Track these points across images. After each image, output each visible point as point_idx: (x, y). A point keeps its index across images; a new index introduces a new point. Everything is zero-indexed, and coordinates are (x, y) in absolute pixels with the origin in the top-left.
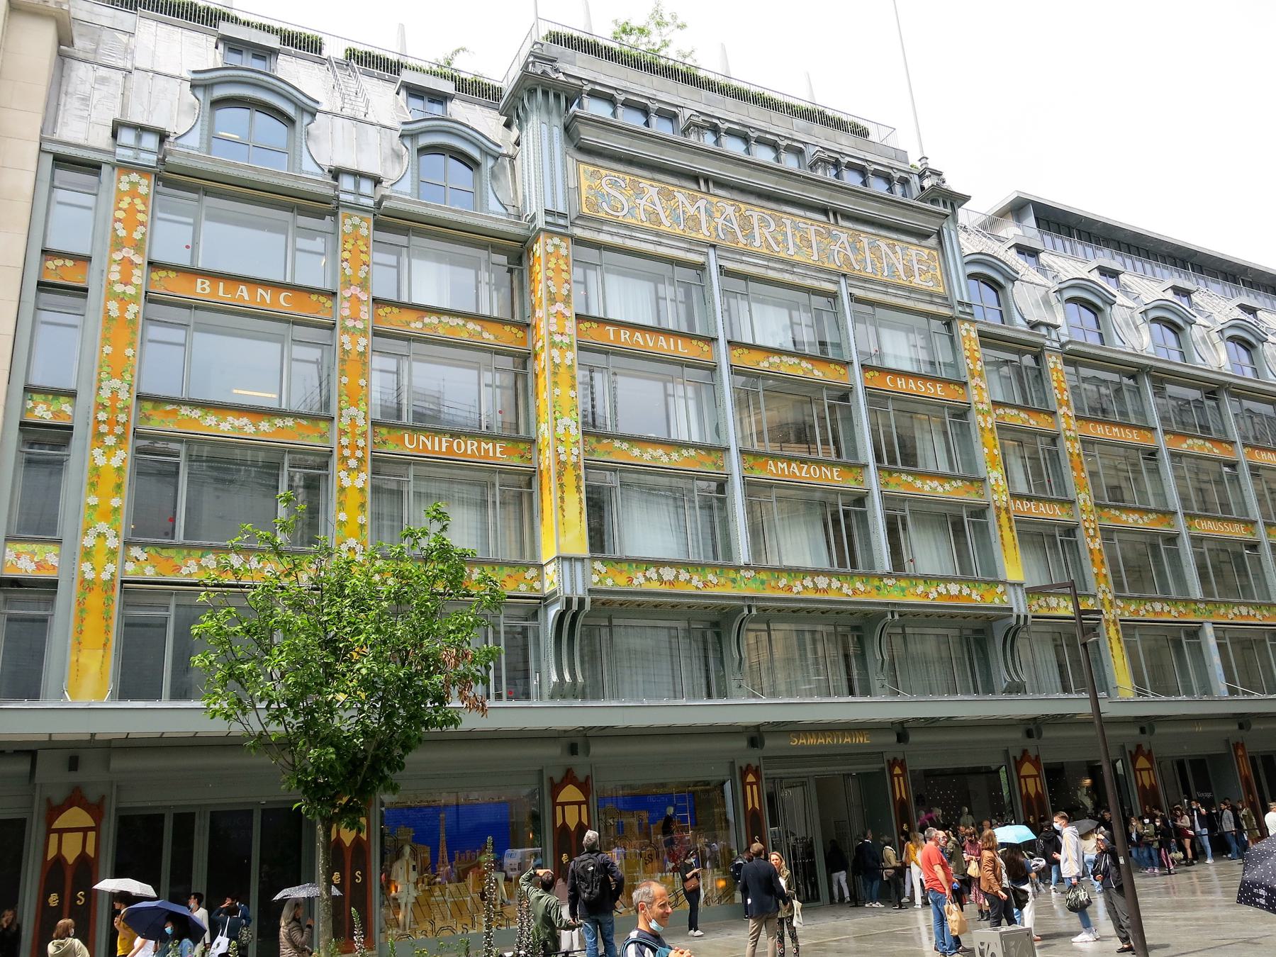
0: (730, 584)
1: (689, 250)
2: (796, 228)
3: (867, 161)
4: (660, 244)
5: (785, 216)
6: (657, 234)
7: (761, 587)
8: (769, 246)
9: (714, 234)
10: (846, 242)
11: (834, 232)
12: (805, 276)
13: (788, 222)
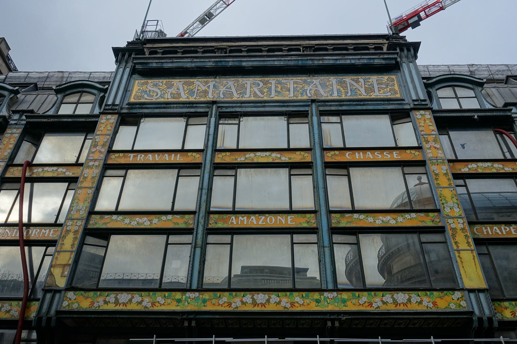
0: (175, 303)
7: (202, 304)
8: (255, 94)
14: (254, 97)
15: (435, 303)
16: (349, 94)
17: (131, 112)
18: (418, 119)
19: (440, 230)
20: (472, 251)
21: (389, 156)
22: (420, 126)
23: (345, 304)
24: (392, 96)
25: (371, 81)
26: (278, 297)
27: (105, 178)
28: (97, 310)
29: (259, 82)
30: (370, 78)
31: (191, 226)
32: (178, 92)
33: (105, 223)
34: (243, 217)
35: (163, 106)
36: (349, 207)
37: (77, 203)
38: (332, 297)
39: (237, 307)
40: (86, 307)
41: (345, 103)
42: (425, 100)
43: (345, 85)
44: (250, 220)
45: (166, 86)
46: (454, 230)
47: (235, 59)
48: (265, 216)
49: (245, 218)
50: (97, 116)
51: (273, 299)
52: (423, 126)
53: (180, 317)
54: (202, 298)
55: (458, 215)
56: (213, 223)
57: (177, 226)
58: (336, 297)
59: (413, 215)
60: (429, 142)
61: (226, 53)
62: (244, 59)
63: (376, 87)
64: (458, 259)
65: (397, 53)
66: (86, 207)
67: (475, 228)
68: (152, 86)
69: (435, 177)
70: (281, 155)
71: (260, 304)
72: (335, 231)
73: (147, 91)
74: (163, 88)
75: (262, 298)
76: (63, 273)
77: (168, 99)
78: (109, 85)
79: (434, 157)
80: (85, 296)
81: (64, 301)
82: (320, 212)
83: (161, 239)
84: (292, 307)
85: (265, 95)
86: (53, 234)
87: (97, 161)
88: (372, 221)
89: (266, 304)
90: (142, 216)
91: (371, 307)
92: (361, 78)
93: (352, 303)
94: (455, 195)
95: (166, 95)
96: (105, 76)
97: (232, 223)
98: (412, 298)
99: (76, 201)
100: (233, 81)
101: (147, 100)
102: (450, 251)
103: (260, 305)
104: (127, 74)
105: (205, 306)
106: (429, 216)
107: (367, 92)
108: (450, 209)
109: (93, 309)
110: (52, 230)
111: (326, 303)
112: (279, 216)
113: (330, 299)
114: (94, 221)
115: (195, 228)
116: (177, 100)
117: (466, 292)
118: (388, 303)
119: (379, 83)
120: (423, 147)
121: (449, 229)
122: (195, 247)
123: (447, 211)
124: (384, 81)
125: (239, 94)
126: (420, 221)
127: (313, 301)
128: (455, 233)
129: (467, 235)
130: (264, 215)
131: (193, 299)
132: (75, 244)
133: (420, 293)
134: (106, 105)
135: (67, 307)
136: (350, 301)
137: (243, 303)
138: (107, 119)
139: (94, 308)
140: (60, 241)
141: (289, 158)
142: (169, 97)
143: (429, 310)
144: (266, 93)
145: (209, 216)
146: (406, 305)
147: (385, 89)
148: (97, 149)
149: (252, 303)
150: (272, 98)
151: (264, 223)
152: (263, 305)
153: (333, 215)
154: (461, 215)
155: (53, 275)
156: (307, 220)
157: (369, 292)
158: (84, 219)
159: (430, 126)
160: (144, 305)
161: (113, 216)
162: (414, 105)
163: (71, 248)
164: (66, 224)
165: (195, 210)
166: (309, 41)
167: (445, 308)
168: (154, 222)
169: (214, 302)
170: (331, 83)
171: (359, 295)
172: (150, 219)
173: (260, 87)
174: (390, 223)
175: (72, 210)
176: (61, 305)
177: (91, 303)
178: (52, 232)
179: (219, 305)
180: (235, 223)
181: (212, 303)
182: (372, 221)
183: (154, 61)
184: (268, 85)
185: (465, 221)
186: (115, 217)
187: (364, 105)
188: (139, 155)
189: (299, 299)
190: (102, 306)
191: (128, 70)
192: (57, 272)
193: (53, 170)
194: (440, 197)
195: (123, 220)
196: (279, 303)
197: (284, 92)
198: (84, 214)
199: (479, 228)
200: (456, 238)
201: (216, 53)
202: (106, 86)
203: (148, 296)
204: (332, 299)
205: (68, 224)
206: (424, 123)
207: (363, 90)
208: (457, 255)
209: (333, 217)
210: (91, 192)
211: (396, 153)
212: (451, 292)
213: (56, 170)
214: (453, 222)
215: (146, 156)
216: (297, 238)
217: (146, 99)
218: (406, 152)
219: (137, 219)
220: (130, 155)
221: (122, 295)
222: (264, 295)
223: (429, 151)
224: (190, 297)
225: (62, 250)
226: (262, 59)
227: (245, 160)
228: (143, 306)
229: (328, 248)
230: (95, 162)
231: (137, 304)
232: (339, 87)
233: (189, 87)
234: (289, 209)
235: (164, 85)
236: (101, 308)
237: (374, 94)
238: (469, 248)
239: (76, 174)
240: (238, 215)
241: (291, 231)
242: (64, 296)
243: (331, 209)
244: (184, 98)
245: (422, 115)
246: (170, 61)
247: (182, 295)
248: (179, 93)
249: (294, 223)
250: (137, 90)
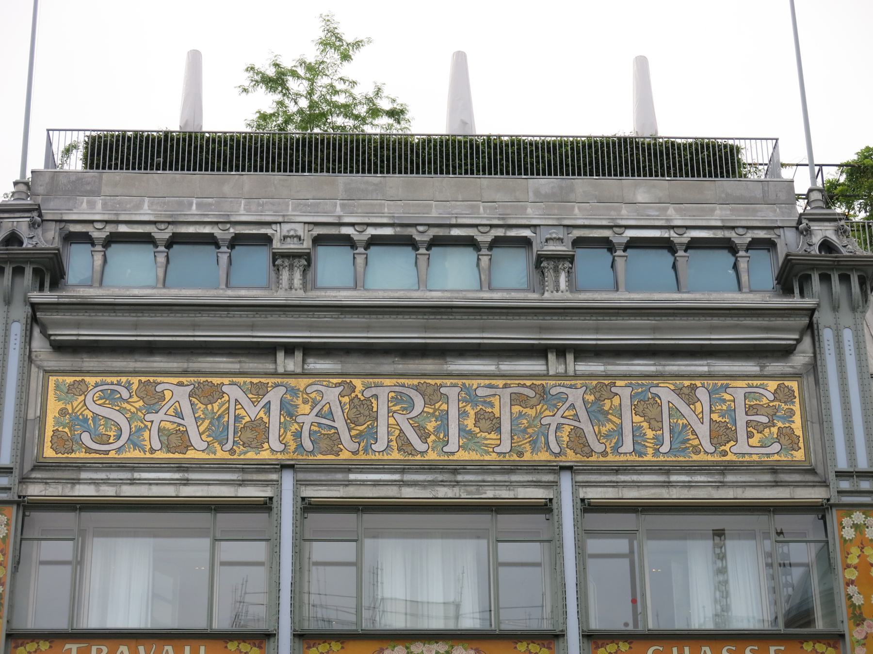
1: (242, 483)
2: (470, 397)
3: (673, 227)
4: (186, 482)
5: (448, 382)
6: (180, 467)
8: (405, 444)
9: (293, 446)
10: (579, 404)
11: (553, 391)
12: (480, 484)
13: (453, 393)
14: (399, 450)
16: (665, 448)
18: (845, 540)
22: (848, 566)
24: (783, 459)
25: (727, 397)
29: (413, 393)
30: (727, 386)
32: (179, 425)
45: (141, 403)
52: (855, 568)
63: (742, 419)
68: (101, 398)
73: (86, 420)
74: (133, 410)
77: (152, 451)
85: (430, 444)
92: (703, 386)
95: (146, 434)
101: (93, 455)
104: (17, 347)
116: (181, 456)
119: (752, 406)
124: (765, 401)
125: (356, 436)
142: (157, 445)
144: (433, 437)
147: (767, 430)
150: (451, 458)
170: (616, 401)
173: (414, 414)
184: (437, 405)
197: (484, 434)
206: (859, 556)
207: (703, 431)
217: (89, 450)
218: (802, 647)
220: (68, 646)
232: (637, 419)
233: (209, 407)
235: (135, 398)
245: (856, 526)
248: (182, 429)
250: (57, 415)
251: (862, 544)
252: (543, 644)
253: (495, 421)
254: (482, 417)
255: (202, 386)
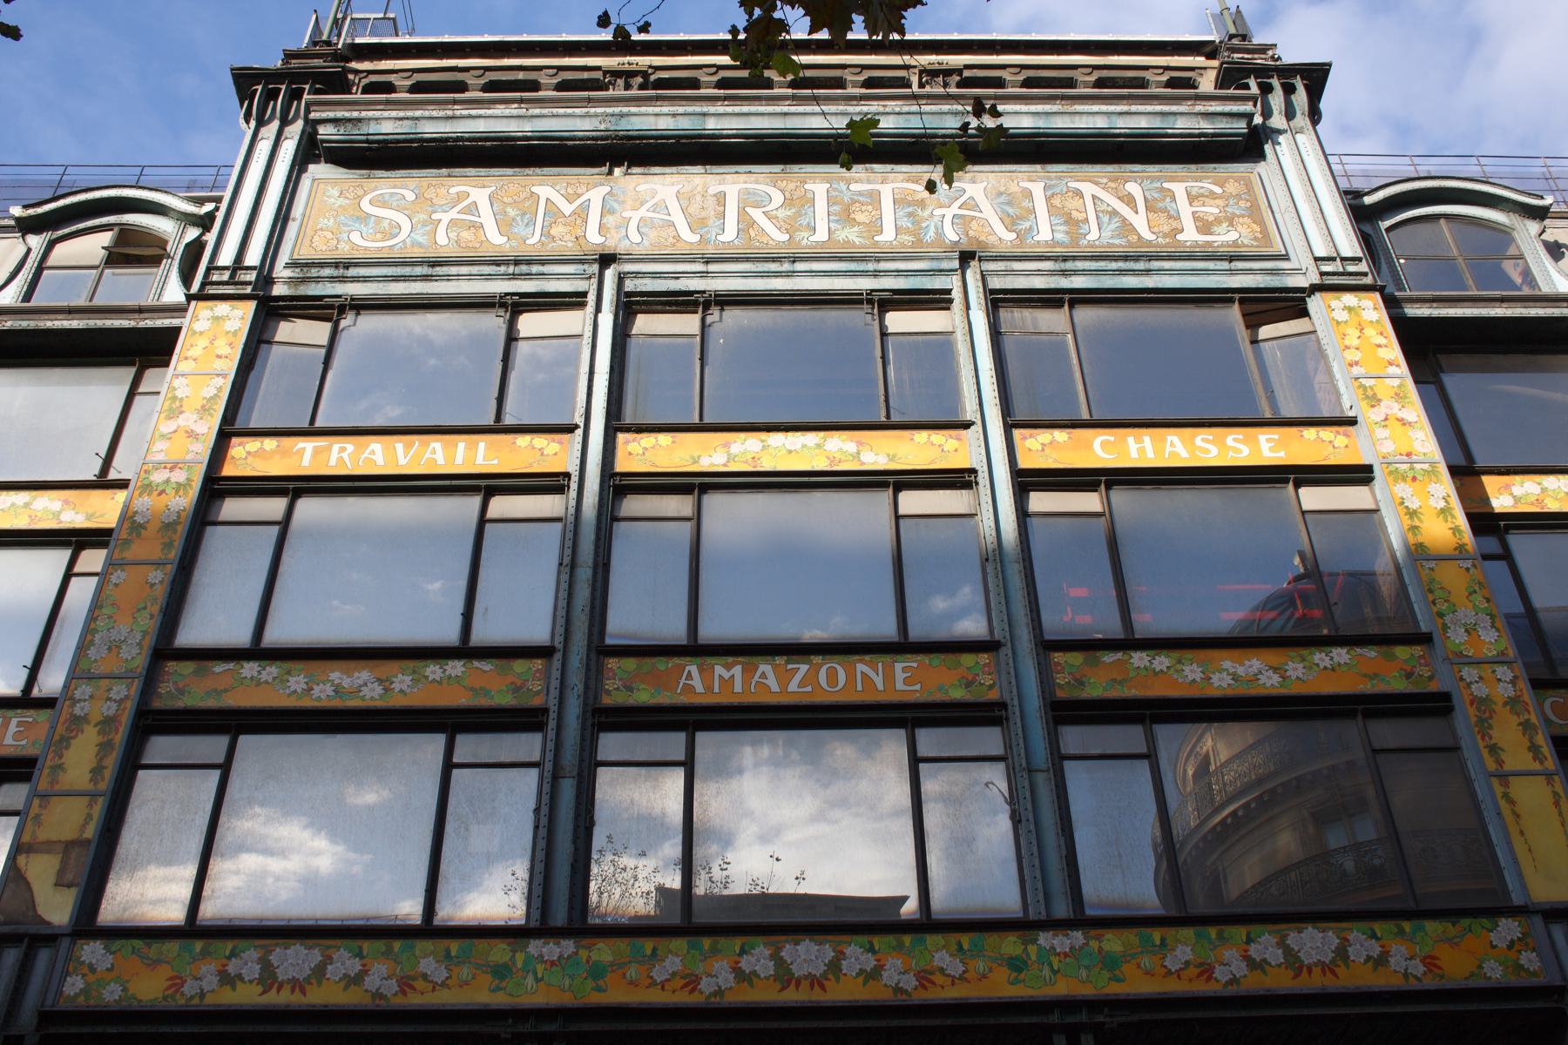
0: (486, 979)
7: (590, 984)
15: (1430, 962)
17: (303, 294)
19: (1438, 705)
20: (1549, 776)
21: (1245, 450)
22: (1347, 347)
23: (1117, 972)
26: (868, 951)
27: (209, 529)
28: (197, 1006)
31: (537, 702)
33: (215, 691)
34: (728, 667)
35: (418, 270)
36: (1111, 626)
37: (110, 617)
38: (1067, 950)
39: (719, 992)
40: (152, 996)
41: (1080, 265)
42: (1358, 260)
43: (1077, 203)
44: (756, 678)
46: (1483, 703)
47: (681, 110)
48: (809, 662)
49: (737, 670)
50: (179, 310)
51: (853, 959)
52: (1357, 349)
53: (509, 1030)
54: (588, 962)
55: (1495, 652)
56: (618, 689)
57: (484, 702)
58: (1081, 948)
59: (1341, 654)
60: (1380, 400)
61: (642, 87)
62: (712, 109)
63: (1185, 210)
64: (1503, 803)
65: (1254, 99)
66: (145, 633)
67: (1547, 704)
69: (1409, 522)
70: (860, 443)
71: (806, 977)
72: (1065, 712)
75: (813, 958)
76: (61, 872)
78: (218, 200)
79: (1401, 454)
80: (148, 958)
81: (68, 974)
82: (1009, 644)
83: (431, 747)
84: (925, 988)
86: (17, 736)
87: (180, 465)
88: (1198, 676)
89: (829, 980)
90: (352, 664)
91: (1210, 978)
93: (1139, 966)
94: (1480, 583)
96: (195, 181)
97: (689, 689)
98: (1350, 945)
99: (105, 611)
100: (673, 185)
102: (1473, 776)
103: (805, 984)
105: (599, 990)
106: (1394, 657)
107: (1156, 230)
108: (1466, 631)
109: (180, 1002)
110: (14, 721)
111: (1046, 972)
112: (861, 661)
113: (1059, 954)
114: (175, 683)
115: (553, 709)
117: (1538, 920)
118: (1269, 964)
120: (1359, 419)
121: (1467, 699)
122: (556, 777)
123: (1457, 637)
126: (1365, 676)
127: (999, 965)
128: (1487, 715)
129: (1527, 721)
130: (806, 658)
131: (553, 963)
132: (106, 768)
133: (1379, 927)
134: (209, 270)
135: (82, 999)
136: (1133, 961)
137: (740, 975)
138: (217, 319)
139: (182, 1002)
140: (50, 757)
141: (888, 456)
143: (1413, 985)
145: (600, 670)
146: (1329, 968)
148: (179, 427)
149: (776, 978)
151: (809, 689)
152: (815, 982)
153: (1058, 657)
154: (1503, 653)
155: (25, 879)
156: (963, 677)
157: (1200, 929)
158: (134, 675)
159: (1380, 346)
160: (369, 988)
161: (242, 667)
162: (1322, 274)
163: (91, 780)
164: (70, 693)
165: (548, 644)
166: (937, 54)
167: (1466, 979)
168: (397, 686)
169: (633, 975)
171: (1163, 940)
172: (384, 677)
174: (1261, 682)
175: (92, 643)
176: (59, 992)
177: (170, 983)
178: (13, 728)
179: (653, 983)
180: (700, 688)
181: (624, 978)
182: (1198, 676)
183: (386, 114)
185: (1518, 674)
186: (251, 669)
187: (1148, 272)
188: (336, 447)
189: (948, 958)
190: (213, 991)
191: (288, 148)
192: (41, 871)
193: (13, 505)
194: (1431, 591)
195: (282, 681)
196: (874, 975)
198: (135, 656)
199: (1562, 700)
200: (1491, 732)
201: (607, 89)
202: (209, 207)
203: (383, 954)
204: (1066, 955)
205: (77, 694)
206: (1359, 337)
208: (1499, 790)
209: (1058, 664)
210: (159, 578)
211: (1268, 440)
212: (1485, 922)
213: (27, 505)
214: (1480, 678)
215: (360, 449)
216: (929, 741)
219: (335, 676)
221: (288, 951)
222: (817, 947)
223: (1381, 433)
224: (541, 956)
225: (57, 787)
226: (778, 109)
227: (728, 461)
228: (366, 991)
229: (1044, 774)
230: (172, 469)
231: (343, 984)
234: (897, 640)
236: (210, 1000)
237: (1179, 237)
238: (1536, 766)
239: (100, 520)
240: (710, 660)
241: (909, 715)
242: (68, 959)
243: (1047, 637)
244: (496, 240)
245: (1350, 309)
246: (441, 114)
247: (514, 951)
249: (918, 687)
251: (1360, 325)
252: (950, 435)
253: (873, 213)
254: (857, 209)
255: (506, 187)
